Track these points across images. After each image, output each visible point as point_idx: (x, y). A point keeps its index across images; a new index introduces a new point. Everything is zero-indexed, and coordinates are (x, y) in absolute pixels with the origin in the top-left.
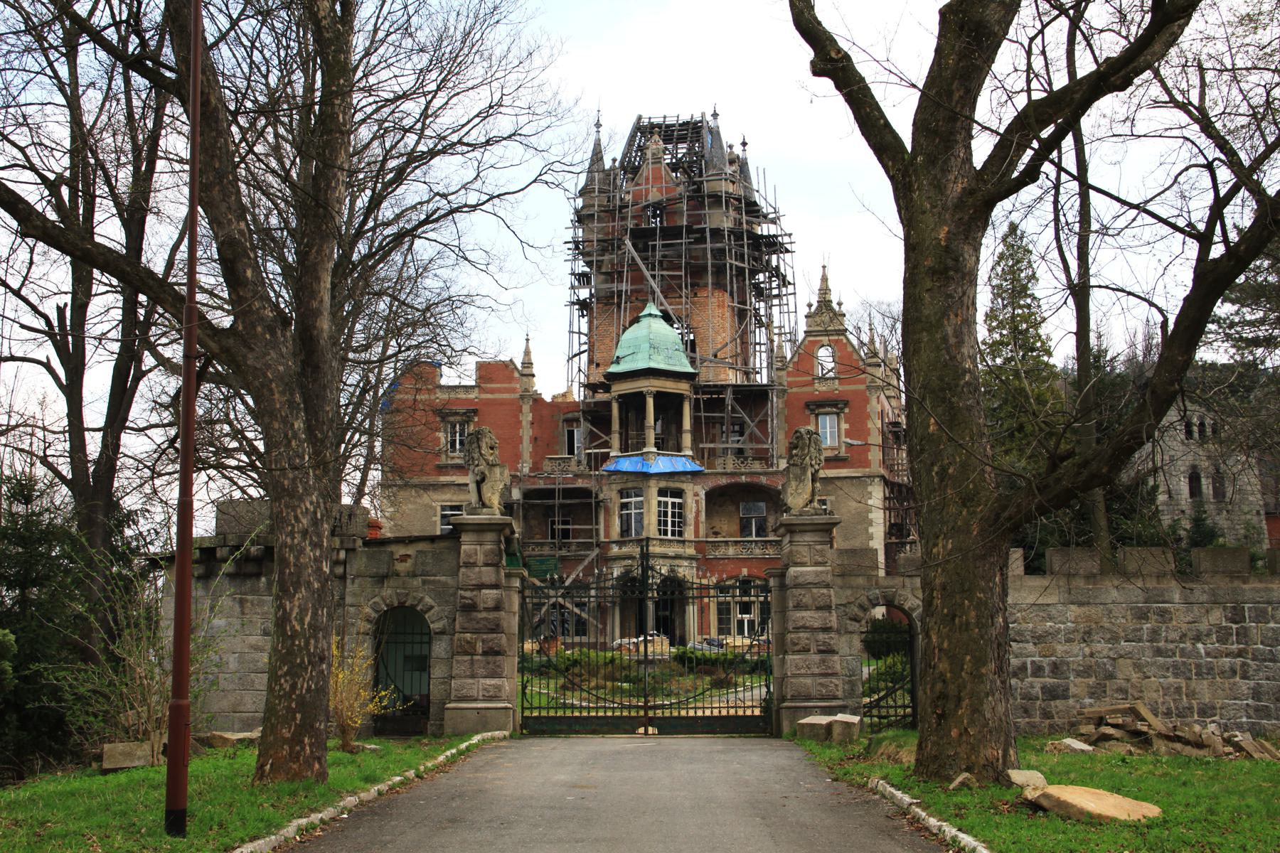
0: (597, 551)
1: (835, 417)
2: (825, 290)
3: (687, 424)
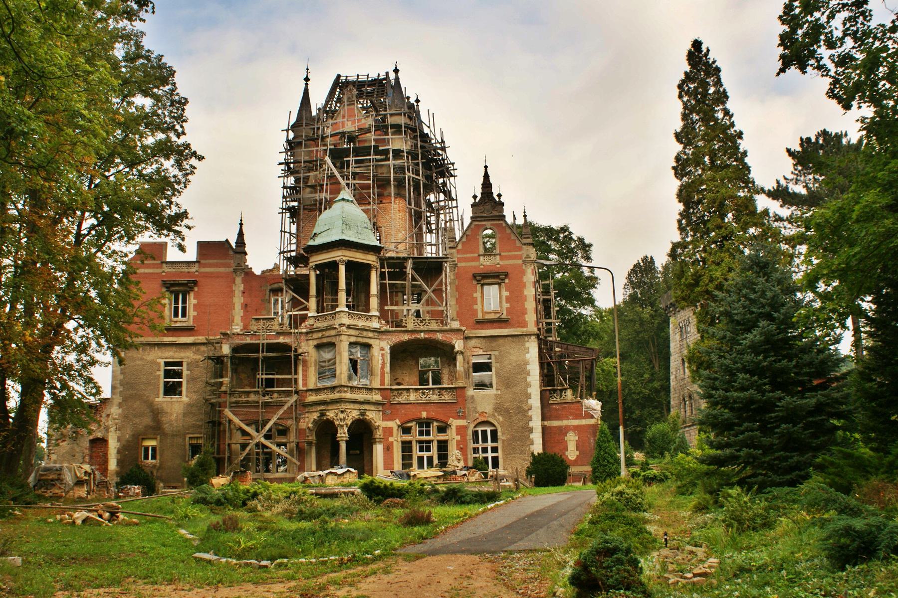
0: (295, 397)
1: (497, 286)
2: (487, 184)
3: (374, 289)
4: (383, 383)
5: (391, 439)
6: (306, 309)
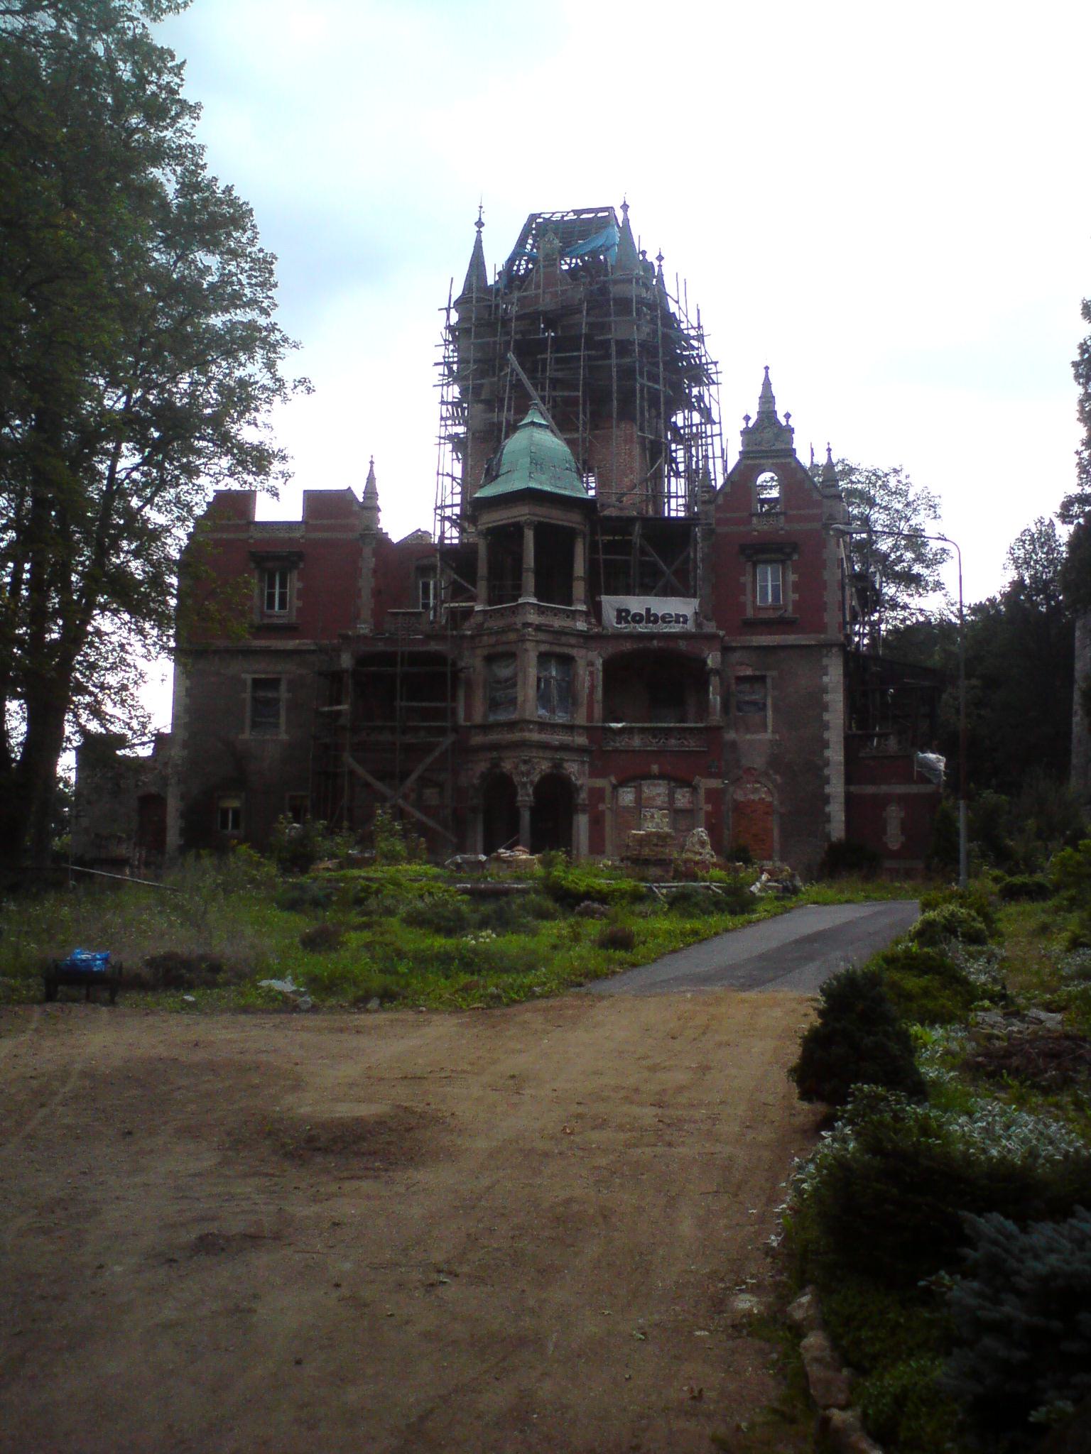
2: (767, 398)
3: (579, 568)
4: (590, 717)
5: (601, 807)
6: (473, 598)
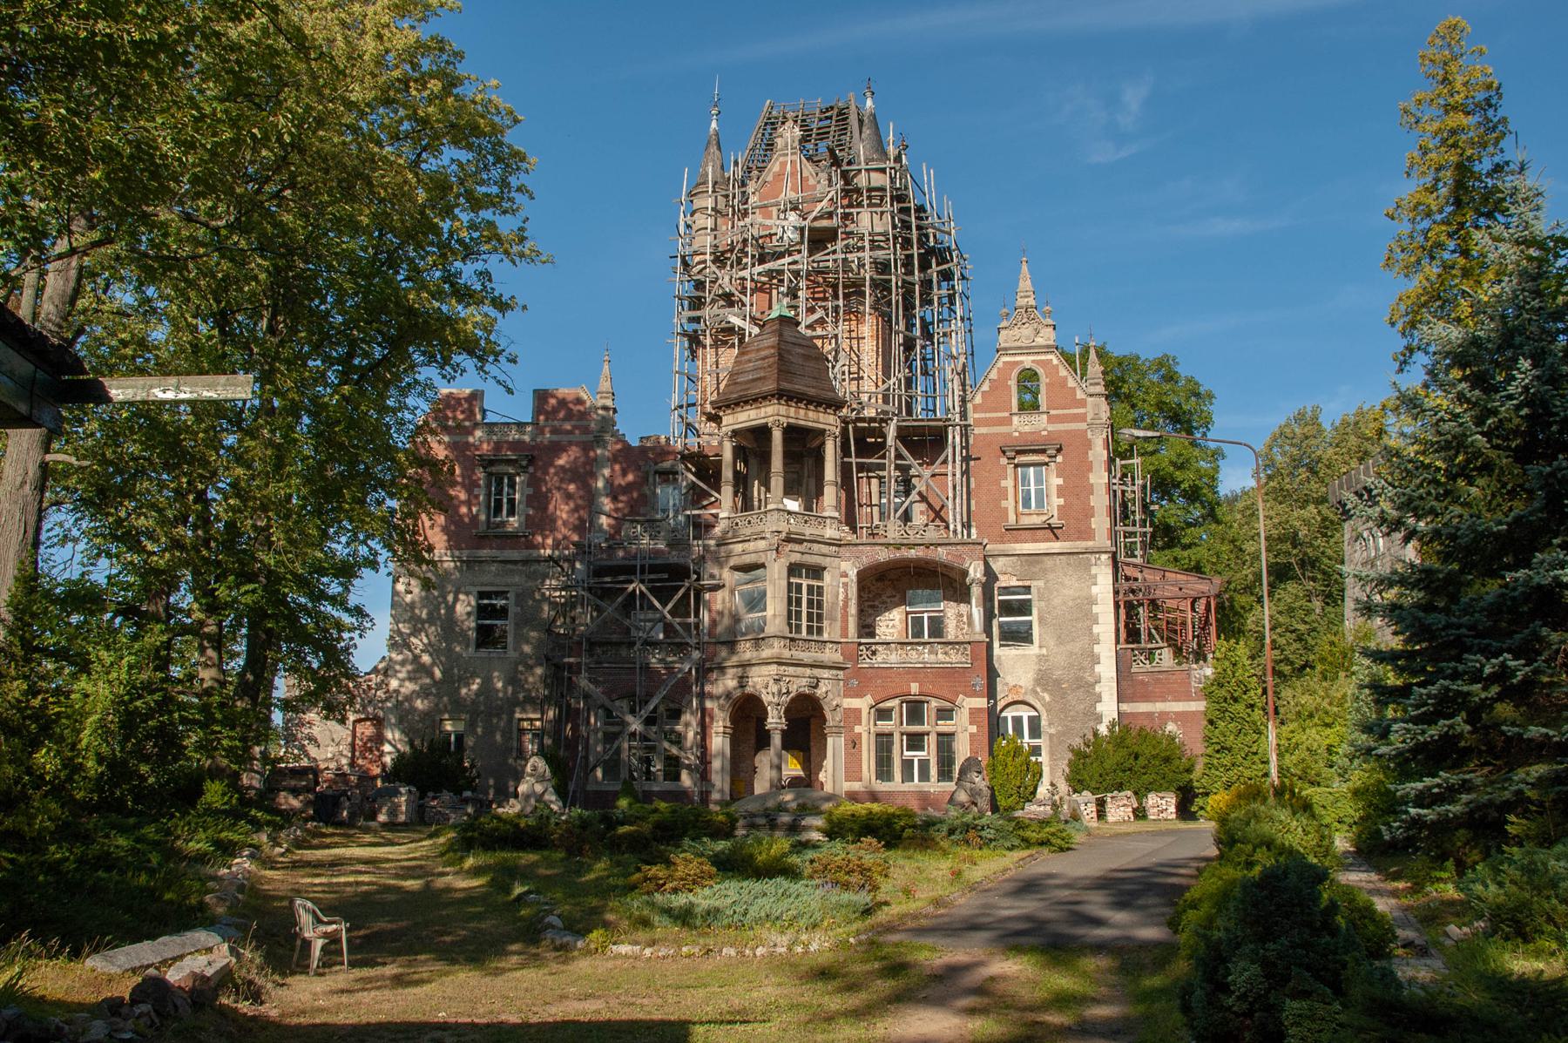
5: (857, 729)
